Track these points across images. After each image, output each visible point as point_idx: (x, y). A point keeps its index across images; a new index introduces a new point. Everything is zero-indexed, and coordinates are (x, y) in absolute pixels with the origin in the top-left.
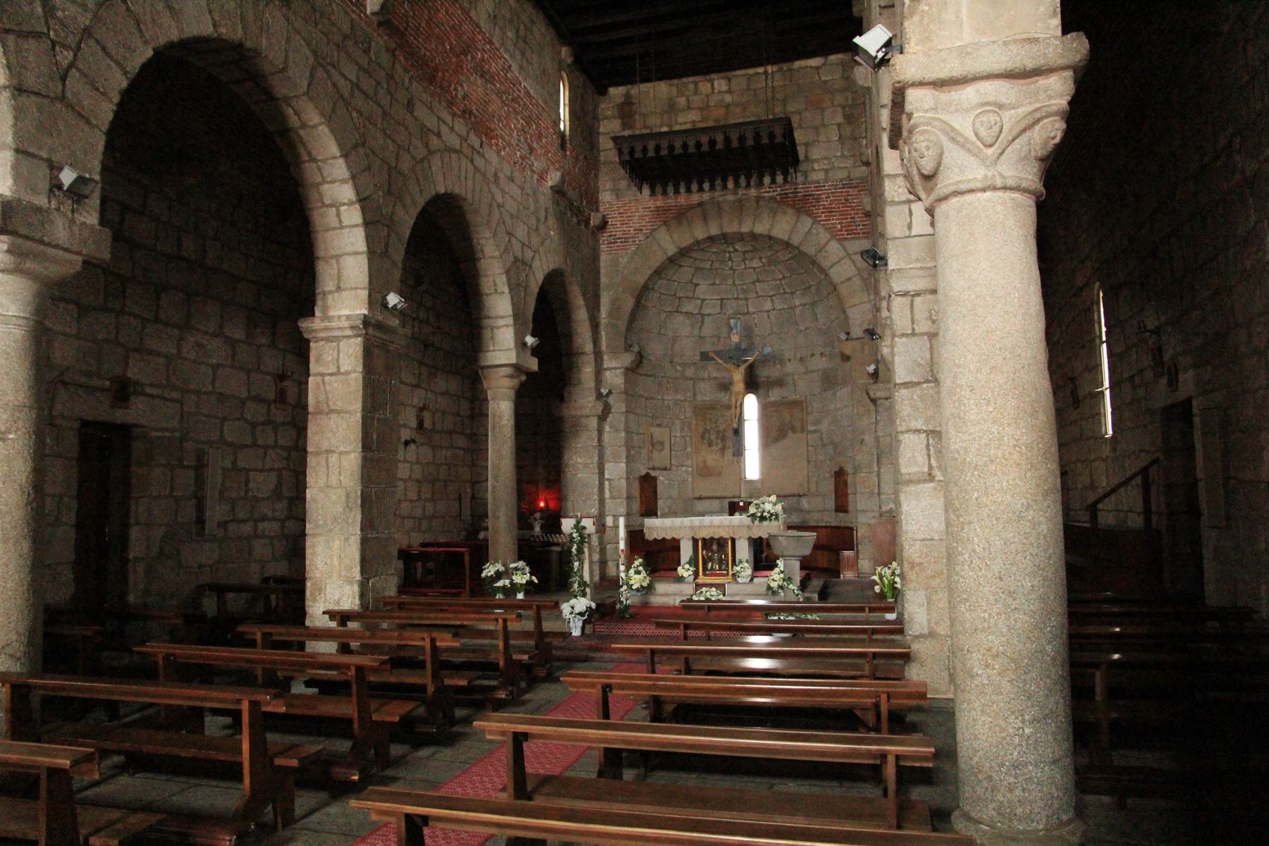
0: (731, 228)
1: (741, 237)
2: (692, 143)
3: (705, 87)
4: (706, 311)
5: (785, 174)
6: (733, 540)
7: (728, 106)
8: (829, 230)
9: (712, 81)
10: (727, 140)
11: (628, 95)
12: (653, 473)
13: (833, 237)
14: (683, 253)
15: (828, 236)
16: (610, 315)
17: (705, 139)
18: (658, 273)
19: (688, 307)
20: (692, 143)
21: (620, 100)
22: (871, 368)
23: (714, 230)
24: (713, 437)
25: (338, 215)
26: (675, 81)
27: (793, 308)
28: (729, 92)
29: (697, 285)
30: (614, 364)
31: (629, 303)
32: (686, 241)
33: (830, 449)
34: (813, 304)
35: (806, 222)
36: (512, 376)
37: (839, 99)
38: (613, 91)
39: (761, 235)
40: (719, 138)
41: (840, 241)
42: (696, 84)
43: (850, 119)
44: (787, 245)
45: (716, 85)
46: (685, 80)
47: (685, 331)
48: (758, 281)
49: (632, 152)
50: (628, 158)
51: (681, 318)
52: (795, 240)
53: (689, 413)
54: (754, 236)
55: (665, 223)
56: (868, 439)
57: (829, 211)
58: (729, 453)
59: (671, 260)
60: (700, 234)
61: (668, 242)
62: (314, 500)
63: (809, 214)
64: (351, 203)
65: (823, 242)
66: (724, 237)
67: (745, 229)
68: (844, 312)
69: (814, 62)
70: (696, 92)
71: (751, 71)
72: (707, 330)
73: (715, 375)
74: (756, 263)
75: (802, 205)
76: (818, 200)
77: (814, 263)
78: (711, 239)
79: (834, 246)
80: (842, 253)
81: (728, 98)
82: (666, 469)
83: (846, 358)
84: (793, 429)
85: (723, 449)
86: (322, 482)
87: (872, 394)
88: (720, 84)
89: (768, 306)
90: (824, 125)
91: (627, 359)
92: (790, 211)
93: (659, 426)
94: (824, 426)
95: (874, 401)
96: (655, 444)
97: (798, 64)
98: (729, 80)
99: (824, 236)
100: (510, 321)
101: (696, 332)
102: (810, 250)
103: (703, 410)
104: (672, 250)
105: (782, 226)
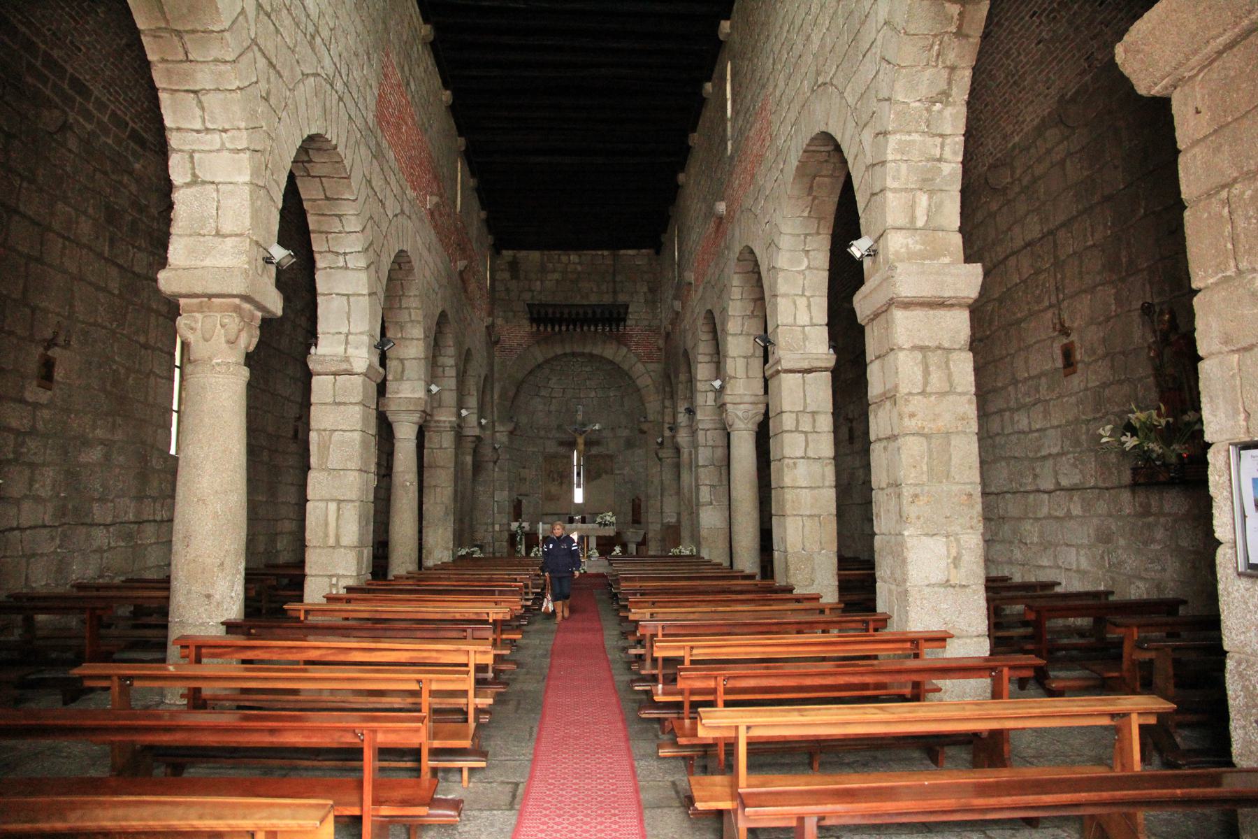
0: (578, 349)
1: (583, 354)
2: (574, 312)
3: (564, 259)
4: (553, 395)
5: (618, 326)
6: (588, 537)
7: (579, 273)
8: (637, 355)
9: (569, 256)
10: (594, 312)
11: (514, 256)
12: (520, 498)
13: (640, 360)
14: (547, 361)
15: (636, 359)
16: (500, 397)
17: (581, 311)
18: (530, 373)
19: (543, 393)
20: (574, 312)
21: (510, 259)
22: (659, 440)
23: (568, 350)
24: (555, 476)
25: (444, 371)
26: (546, 252)
27: (608, 397)
28: (579, 263)
29: (549, 379)
30: (502, 429)
31: (511, 394)
32: (551, 355)
33: (629, 486)
34: (622, 397)
35: (624, 350)
36: (473, 442)
37: (646, 277)
38: (505, 252)
39: (597, 355)
40: (590, 312)
41: (644, 363)
42: (559, 255)
43: (652, 290)
44: (611, 362)
45: (572, 258)
46: (552, 252)
47: (540, 407)
48: (589, 379)
49: (539, 313)
50: (535, 316)
51: (539, 400)
52: (618, 360)
53: (541, 459)
54: (591, 355)
55: (538, 342)
56: (656, 481)
57: (637, 343)
58: (564, 487)
59: (539, 366)
60: (559, 351)
61: (539, 355)
62: (428, 509)
63: (626, 345)
64: (451, 366)
65: (633, 362)
66: (574, 354)
67: (587, 350)
68: (643, 404)
69: (631, 252)
70: (559, 261)
71: (594, 252)
72: (553, 408)
73: (557, 435)
74: (588, 369)
75: (622, 340)
76: (631, 337)
77: (627, 374)
78: (565, 354)
79: (639, 365)
80: (644, 371)
81: (579, 268)
82: (527, 495)
83: (642, 432)
84: (606, 473)
85: (561, 484)
86: (432, 501)
87: (660, 455)
88: (574, 258)
89: (593, 394)
90: (636, 292)
91: (510, 426)
92: (614, 342)
93: (524, 468)
94: (627, 470)
95: (660, 459)
96: (523, 480)
97: (622, 252)
98: (580, 256)
99: (634, 359)
100: (476, 411)
101: (547, 408)
102: (626, 367)
103: (549, 458)
104: (540, 359)
105: (609, 351)
